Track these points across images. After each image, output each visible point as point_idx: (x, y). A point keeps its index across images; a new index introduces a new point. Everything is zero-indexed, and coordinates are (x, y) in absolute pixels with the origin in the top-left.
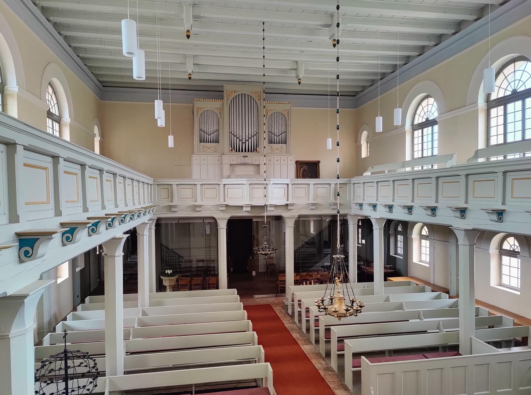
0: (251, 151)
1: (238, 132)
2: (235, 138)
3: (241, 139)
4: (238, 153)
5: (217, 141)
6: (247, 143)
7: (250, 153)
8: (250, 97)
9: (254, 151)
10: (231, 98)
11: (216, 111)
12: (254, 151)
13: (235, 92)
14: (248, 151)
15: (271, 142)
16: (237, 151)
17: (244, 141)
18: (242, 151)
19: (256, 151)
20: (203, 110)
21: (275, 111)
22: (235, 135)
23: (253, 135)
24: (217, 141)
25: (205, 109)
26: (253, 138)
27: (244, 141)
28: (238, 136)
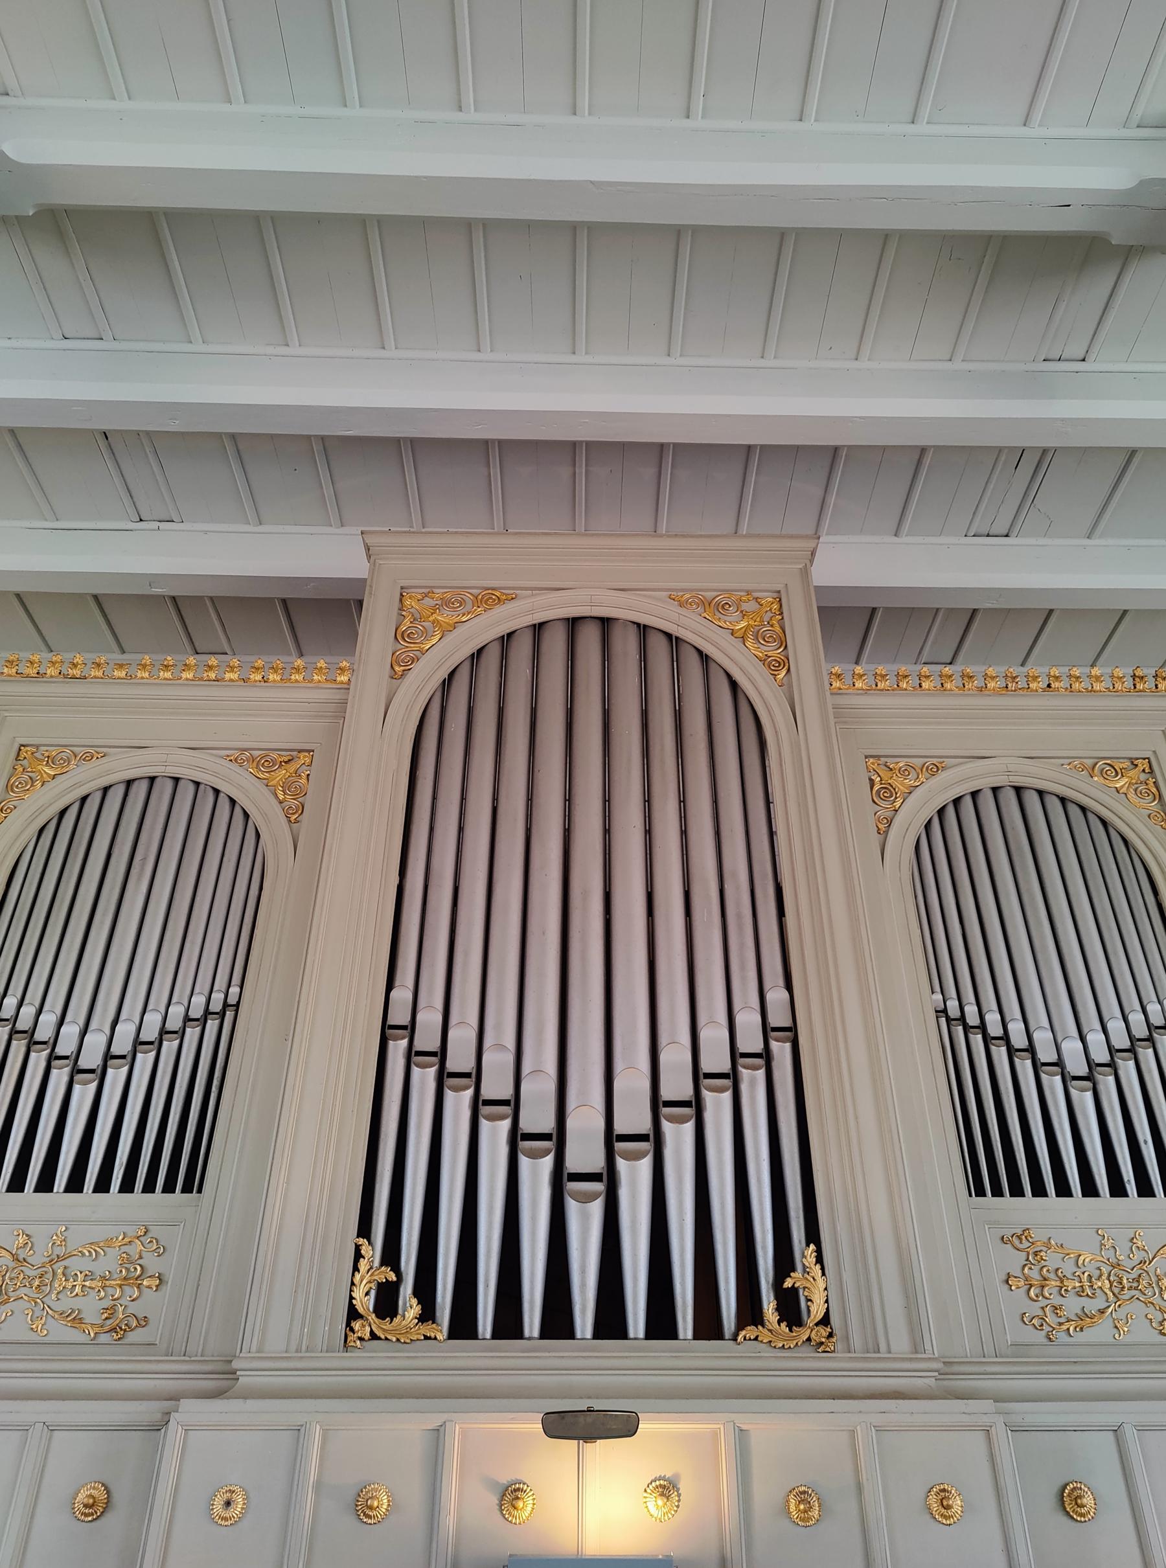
0: (708, 1326)
1: (502, 1028)
2: (458, 1103)
3: (538, 1116)
4: (484, 1356)
5: (184, 1170)
6: (635, 1178)
7: (686, 1351)
8: (659, 652)
9: (750, 1313)
10: (443, 653)
11: (242, 785)
12: (750, 1313)
13: (490, 598)
14: (661, 1324)
15: (1000, 1162)
16: (463, 1326)
17: (584, 1153)
18: (557, 1323)
19: (791, 1309)
20: (85, 778)
21: (981, 776)
22: (460, 1059)
23: (716, 1059)
24: (184, 1170)
25: (119, 768)
26: (717, 1105)
27: (584, 1153)
28: (496, 1085)
